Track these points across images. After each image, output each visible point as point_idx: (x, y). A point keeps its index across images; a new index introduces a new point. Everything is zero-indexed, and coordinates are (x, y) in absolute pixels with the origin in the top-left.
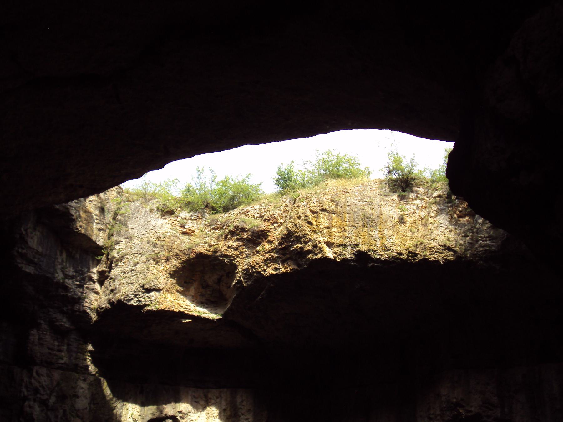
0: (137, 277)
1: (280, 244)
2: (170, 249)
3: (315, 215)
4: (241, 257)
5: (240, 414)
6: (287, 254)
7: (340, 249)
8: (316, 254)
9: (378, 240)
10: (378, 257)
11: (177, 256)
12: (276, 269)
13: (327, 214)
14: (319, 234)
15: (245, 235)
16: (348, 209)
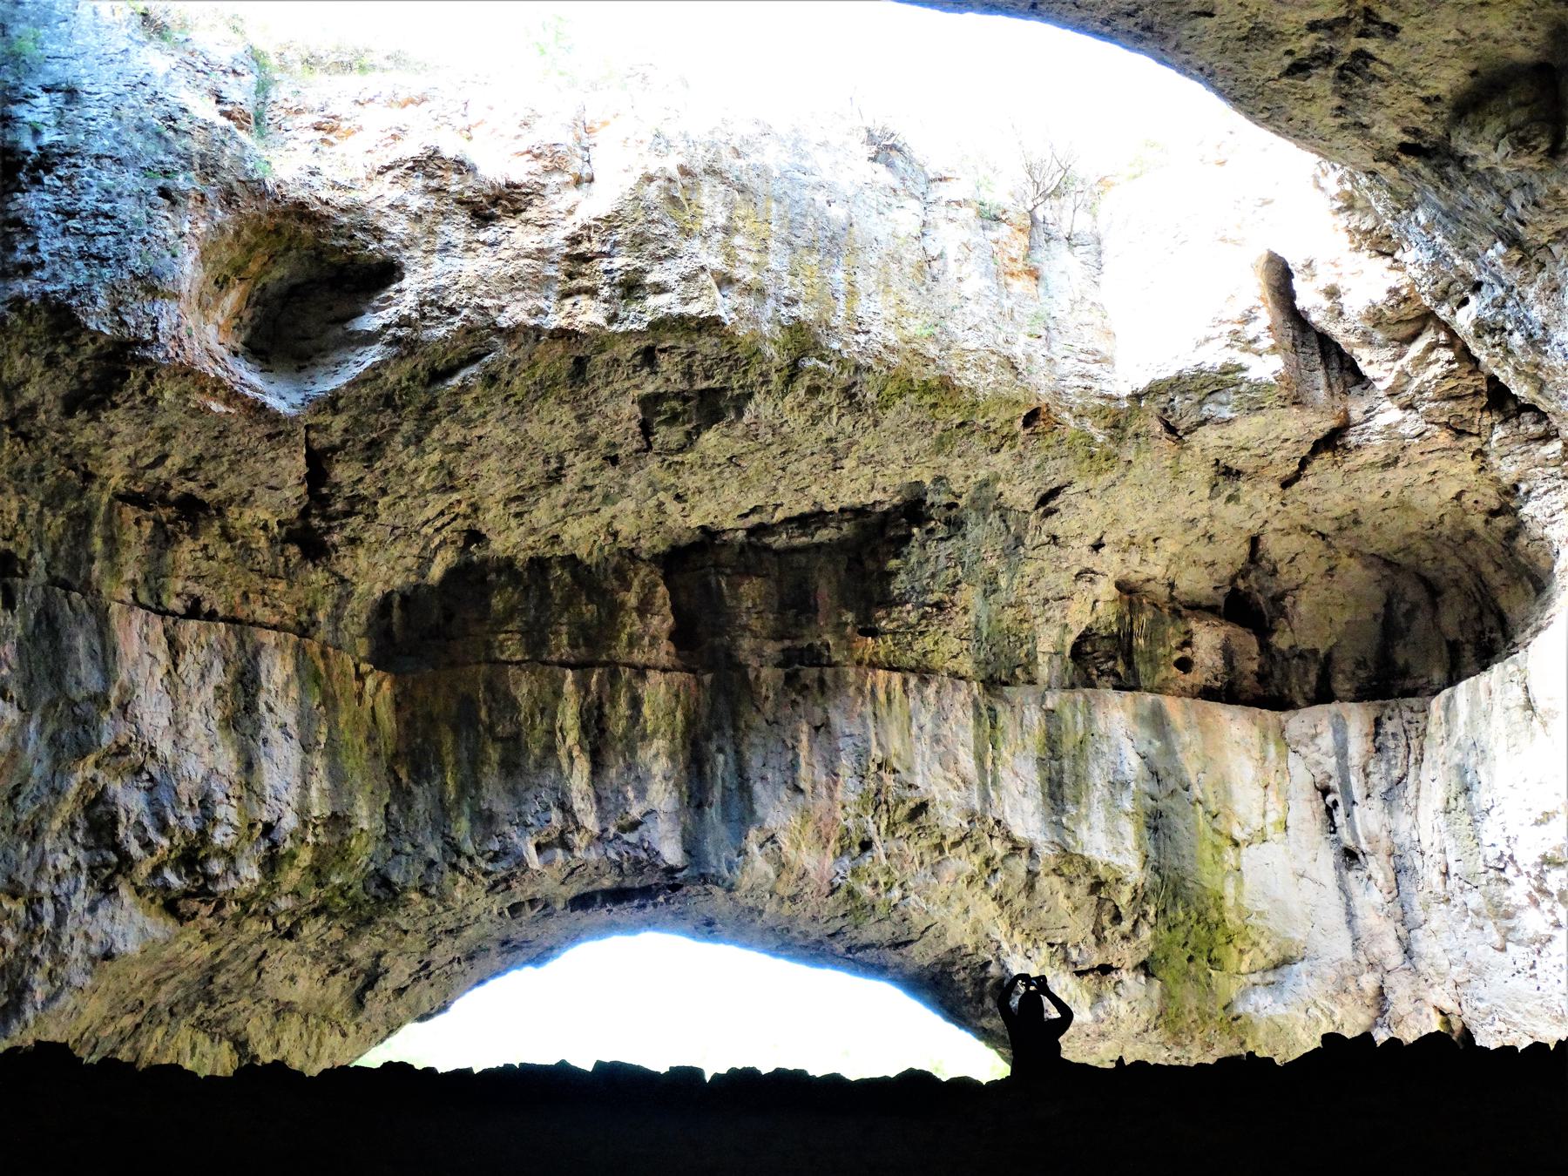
0: (120, 242)
1: (574, 240)
2: (209, 169)
3: (686, 181)
4: (424, 247)
5: (262, 708)
6: (582, 275)
7: (749, 303)
8: (686, 301)
9: (842, 298)
10: (836, 345)
11: (229, 198)
12: (541, 311)
13: (722, 188)
14: (697, 243)
15: (454, 183)
16: (778, 189)
